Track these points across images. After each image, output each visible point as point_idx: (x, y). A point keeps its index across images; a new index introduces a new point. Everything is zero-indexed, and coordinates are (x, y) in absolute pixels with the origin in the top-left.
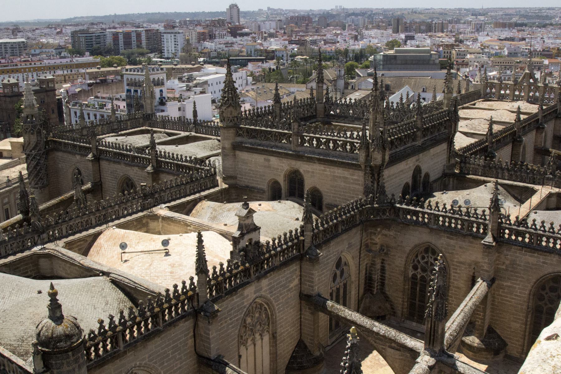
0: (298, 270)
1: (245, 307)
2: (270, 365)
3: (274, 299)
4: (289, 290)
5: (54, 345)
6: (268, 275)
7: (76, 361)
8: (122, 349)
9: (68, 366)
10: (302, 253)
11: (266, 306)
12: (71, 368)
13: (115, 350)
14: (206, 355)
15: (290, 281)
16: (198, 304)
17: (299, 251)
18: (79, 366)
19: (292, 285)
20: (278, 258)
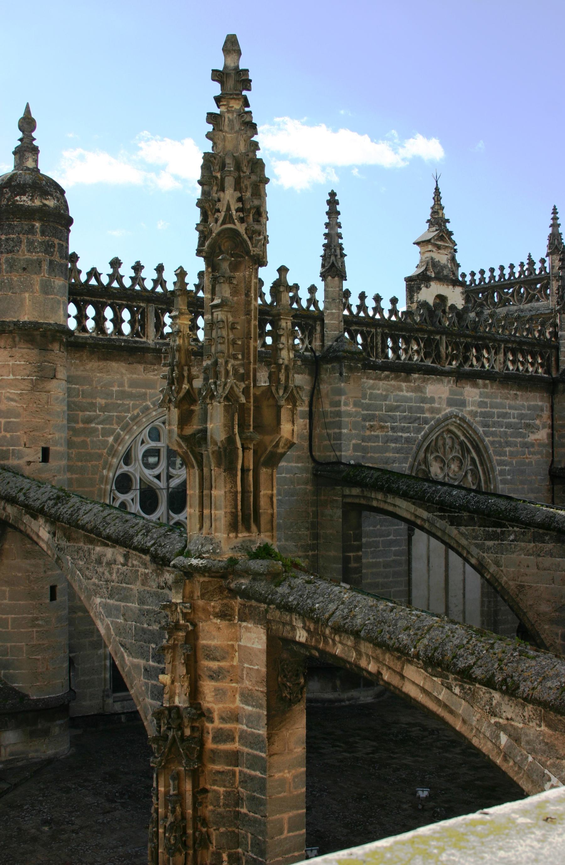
0: (546, 414)
1: (426, 421)
2: (482, 606)
3: (492, 443)
4: (526, 445)
5: (8, 200)
6: (480, 382)
7: (48, 248)
8: (150, 342)
9: (29, 251)
10: (554, 376)
11: (474, 455)
12: (34, 256)
13: (137, 339)
14: (331, 456)
15: (528, 426)
16: (323, 346)
17: (548, 371)
18: (51, 262)
19: (532, 438)
20: (501, 357)
